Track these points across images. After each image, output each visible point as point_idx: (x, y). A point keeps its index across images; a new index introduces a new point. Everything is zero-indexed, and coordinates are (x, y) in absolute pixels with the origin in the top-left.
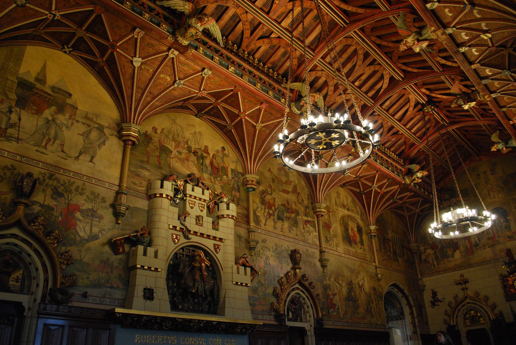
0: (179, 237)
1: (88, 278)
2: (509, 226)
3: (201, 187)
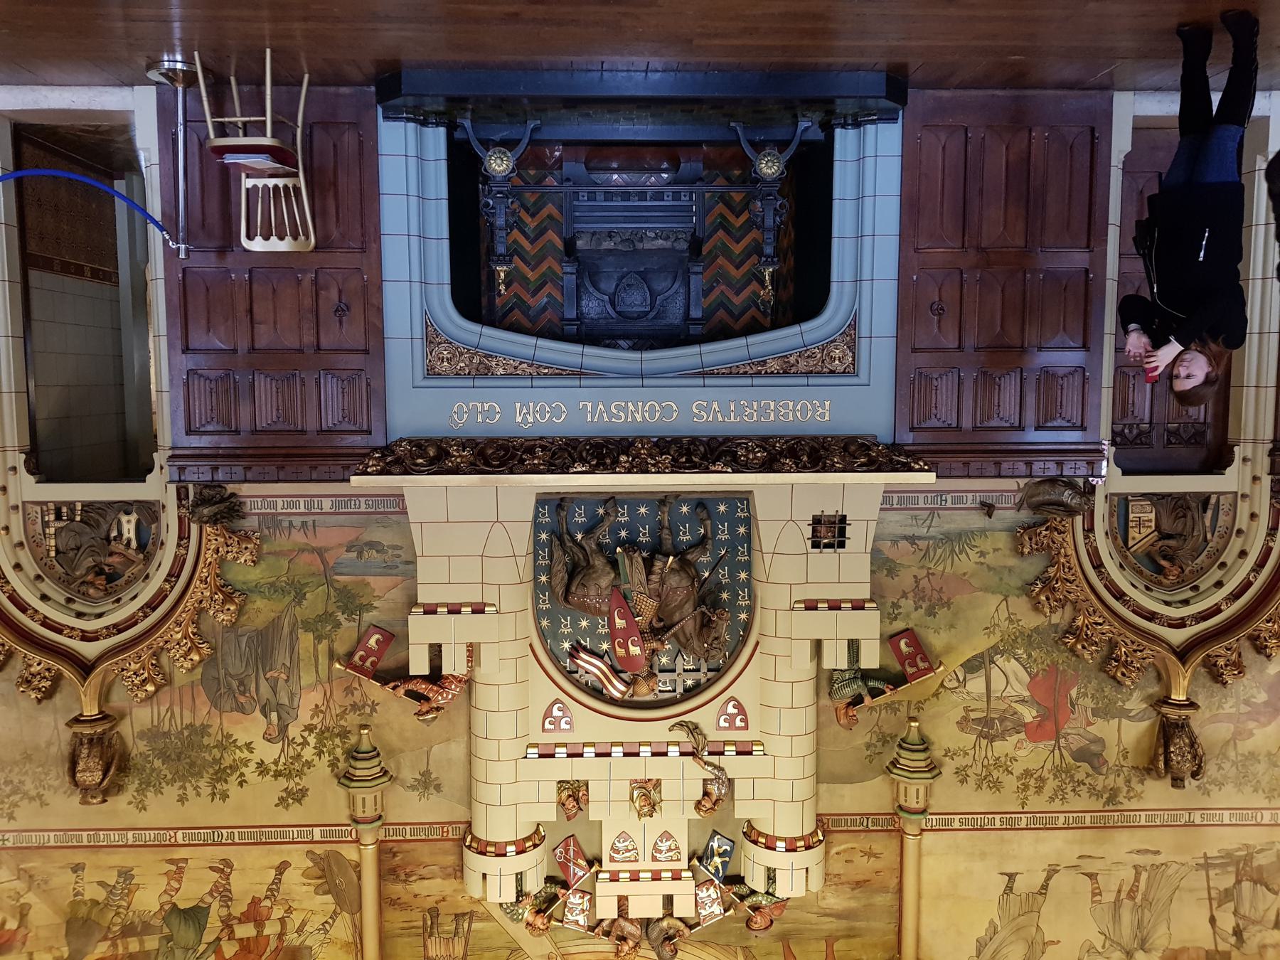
0: (722, 723)
1: (982, 554)
3: (631, 921)
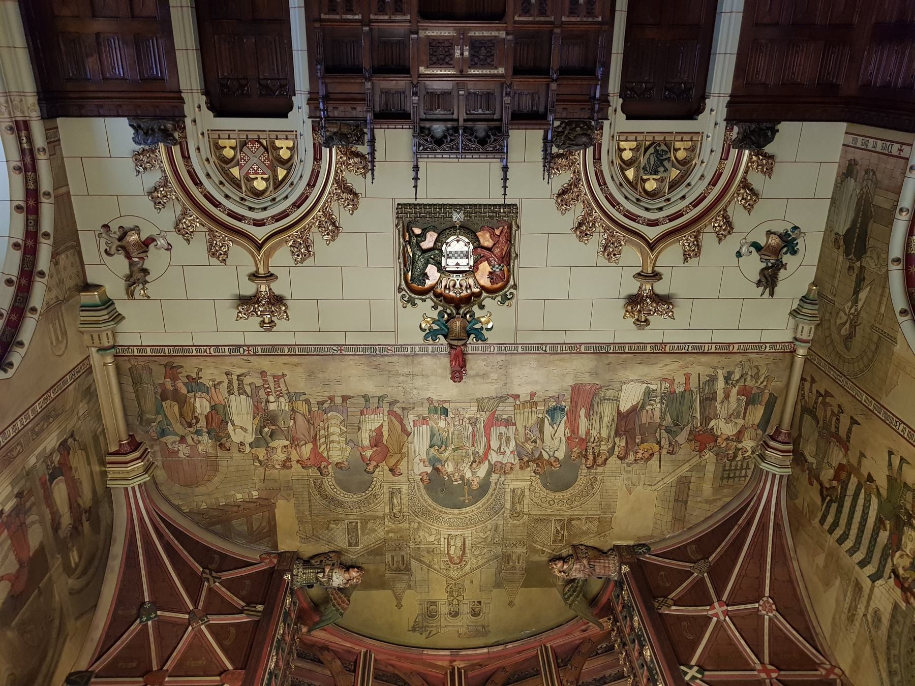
2: (431, 447)
